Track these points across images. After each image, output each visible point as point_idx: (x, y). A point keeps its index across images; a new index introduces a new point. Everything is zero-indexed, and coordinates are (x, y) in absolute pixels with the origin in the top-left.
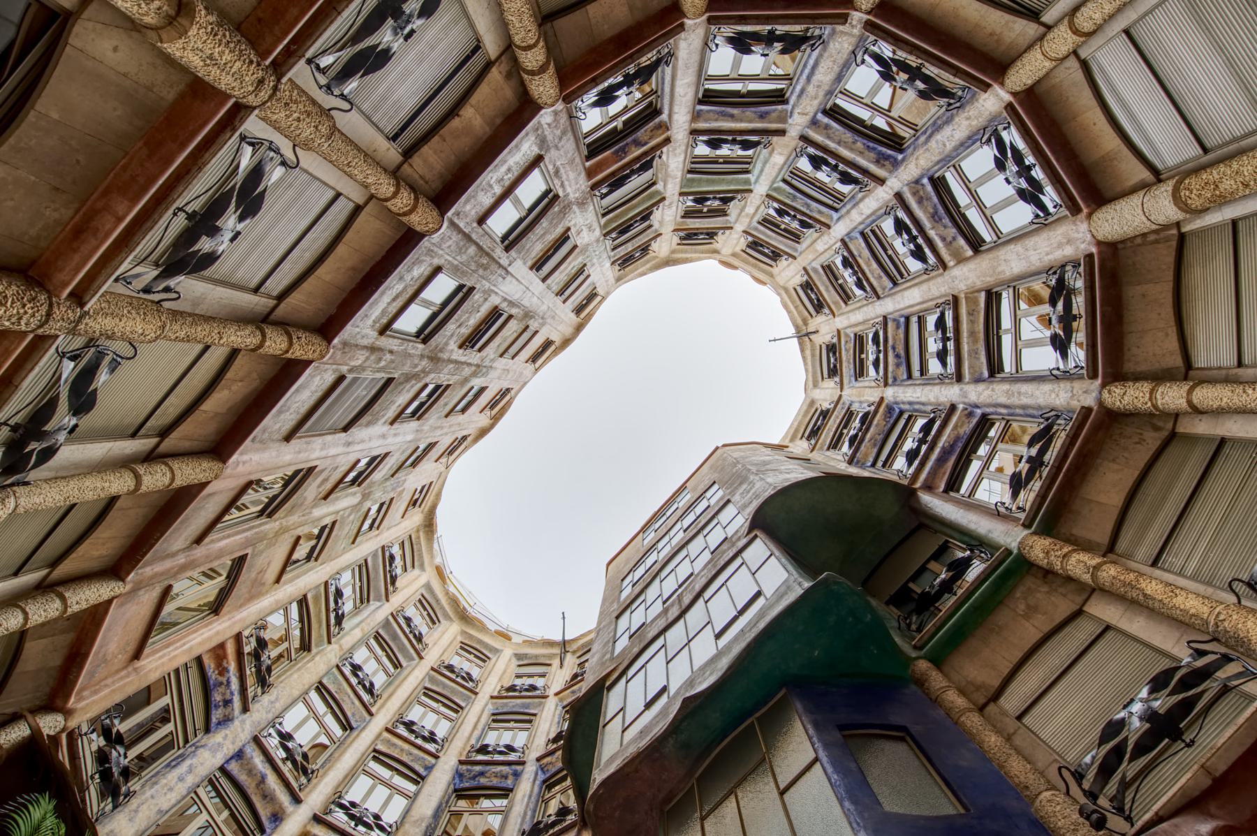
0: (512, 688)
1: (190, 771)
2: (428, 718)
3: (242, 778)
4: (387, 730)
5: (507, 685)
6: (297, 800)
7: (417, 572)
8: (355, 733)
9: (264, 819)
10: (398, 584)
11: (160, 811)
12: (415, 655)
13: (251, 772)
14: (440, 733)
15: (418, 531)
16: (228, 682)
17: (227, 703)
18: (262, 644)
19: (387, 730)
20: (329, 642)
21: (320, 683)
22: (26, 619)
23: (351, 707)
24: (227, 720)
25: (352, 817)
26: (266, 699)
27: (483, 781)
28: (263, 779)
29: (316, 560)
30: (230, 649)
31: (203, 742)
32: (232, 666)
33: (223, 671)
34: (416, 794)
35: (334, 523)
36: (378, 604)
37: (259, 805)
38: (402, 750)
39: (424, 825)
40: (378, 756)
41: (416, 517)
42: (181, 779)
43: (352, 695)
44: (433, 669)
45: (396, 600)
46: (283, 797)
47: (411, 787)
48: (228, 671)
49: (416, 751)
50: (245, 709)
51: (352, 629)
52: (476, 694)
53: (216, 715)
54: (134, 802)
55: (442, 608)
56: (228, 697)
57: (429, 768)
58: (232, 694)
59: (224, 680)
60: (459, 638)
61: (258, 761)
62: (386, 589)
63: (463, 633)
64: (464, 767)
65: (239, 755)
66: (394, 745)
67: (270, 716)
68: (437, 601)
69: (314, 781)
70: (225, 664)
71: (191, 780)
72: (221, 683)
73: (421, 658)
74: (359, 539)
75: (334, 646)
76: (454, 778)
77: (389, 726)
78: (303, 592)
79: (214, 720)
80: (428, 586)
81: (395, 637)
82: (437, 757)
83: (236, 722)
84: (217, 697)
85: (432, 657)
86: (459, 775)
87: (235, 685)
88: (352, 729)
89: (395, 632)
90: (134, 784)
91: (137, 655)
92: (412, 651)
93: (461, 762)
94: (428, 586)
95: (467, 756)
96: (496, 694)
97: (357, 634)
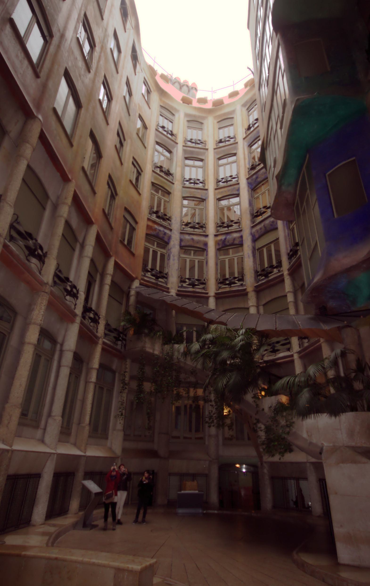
0: (249, 128)
1: (174, 256)
2: (226, 172)
3: (188, 244)
4: (216, 189)
5: (246, 127)
6: (207, 236)
7: (177, 115)
8: (207, 200)
9: (203, 247)
10: (174, 132)
11: (177, 270)
12: (204, 151)
13: (188, 241)
14: (234, 174)
15: (161, 100)
16: (160, 230)
17: (165, 234)
18: (157, 212)
19: (216, 189)
20: (173, 184)
21: (183, 197)
22: (108, 284)
23: (199, 194)
24: (170, 238)
25: (225, 227)
26: (173, 221)
27: (259, 180)
28: (193, 239)
29: (142, 171)
30: (150, 224)
31: (170, 248)
32: (156, 226)
33: (155, 229)
34: (240, 202)
35: (134, 158)
36: (175, 149)
37: (198, 246)
38: (225, 191)
39: (248, 212)
40: (219, 199)
41: (155, 97)
42: (174, 260)
43: (196, 190)
44: (215, 149)
45: (180, 140)
46: (203, 239)
47: (236, 200)
48: (156, 228)
49: (230, 188)
50: (171, 230)
51: (176, 170)
52: (237, 143)
53: (166, 239)
54: (170, 274)
55: (199, 117)
56: (163, 233)
57: (238, 190)
58: (164, 231)
59: (158, 231)
60: (216, 121)
61: (187, 237)
62: (173, 141)
63: (215, 118)
64: (250, 180)
65: (181, 240)
66: (222, 192)
67: (179, 224)
68: (195, 116)
69: (207, 226)
70: (153, 228)
71: (176, 258)
72: (158, 232)
73: (207, 149)
74: (146, 145)
75: (176, 183)
76: (249, 186)
77: (216, 188)
78: (150, 182)
79: (166, 240)
80: (187, 115)
81: (192, 152)
82: (238, 184)
83: (172, 235)
84: (161, 235)
85: (211, 145)
86: (249, 184)
87: (162, 229)
88: (205, 200)
89: (190, 151)
90: (166, 271)
91: (133, 255)
92: (202, 150)
93: (247, 179)
94: (187, 115)
95: (249, 174)
96: (245, 136)
97: (179, 170)
